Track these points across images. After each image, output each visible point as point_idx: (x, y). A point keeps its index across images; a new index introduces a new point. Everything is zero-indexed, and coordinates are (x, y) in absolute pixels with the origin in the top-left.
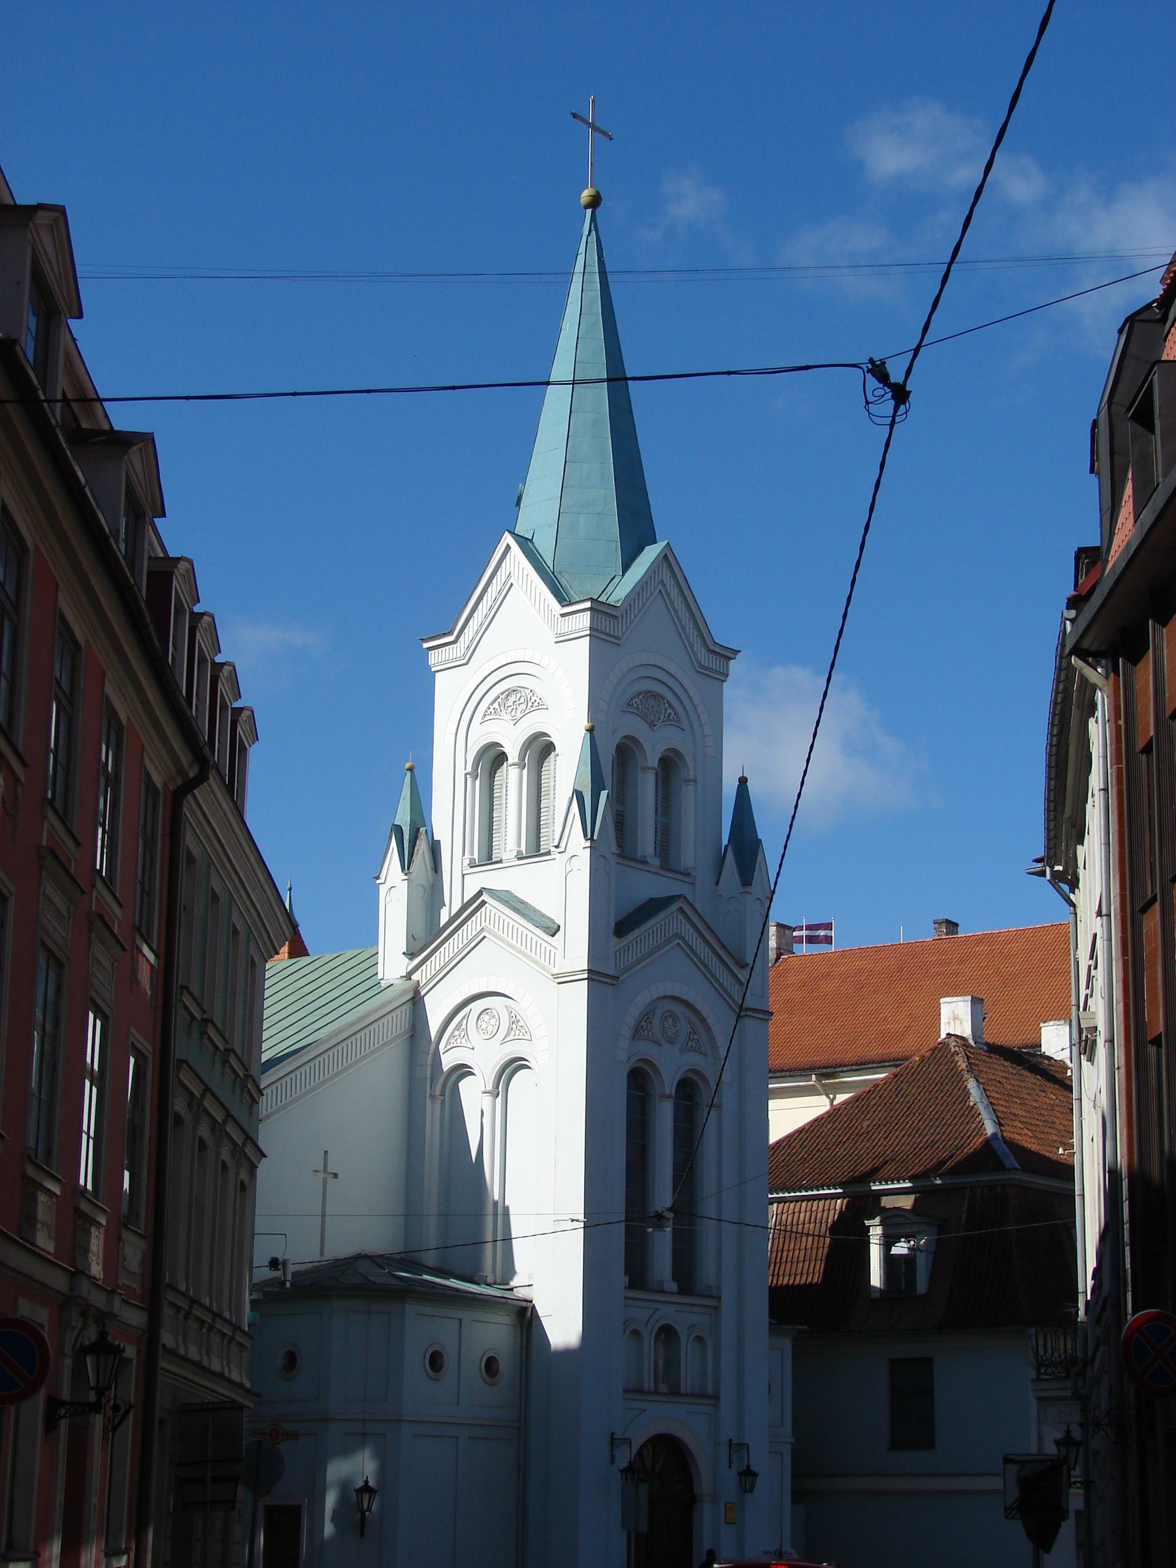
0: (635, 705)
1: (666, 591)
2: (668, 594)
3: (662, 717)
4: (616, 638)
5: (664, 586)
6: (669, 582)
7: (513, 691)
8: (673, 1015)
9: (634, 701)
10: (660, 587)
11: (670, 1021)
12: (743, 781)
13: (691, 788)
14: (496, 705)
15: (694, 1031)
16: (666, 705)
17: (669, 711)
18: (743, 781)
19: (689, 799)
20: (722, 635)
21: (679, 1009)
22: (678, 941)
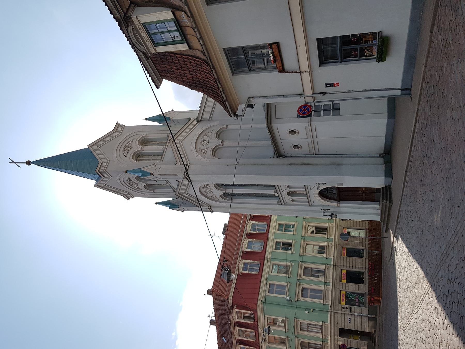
0: (126, 154)
1: (100, 146)
2: (100, 145)
3: (130, 145)
4: (107, 162)
5: (98, 146)
6: (98, 144)
7: (129, 184)
8: (201, 143)
9: (125, 155)
10: (99, 147)
11: (203, 143)
12: (146, 119)
13: (149, 135)
14: (135, 187)
15: (206, 135)
16: (127, 144)
17: (129, 143)
18: (146, 119)
19: (151, 136)
20: (111, 128)
21: (200, 140)
22: (181, 142)
